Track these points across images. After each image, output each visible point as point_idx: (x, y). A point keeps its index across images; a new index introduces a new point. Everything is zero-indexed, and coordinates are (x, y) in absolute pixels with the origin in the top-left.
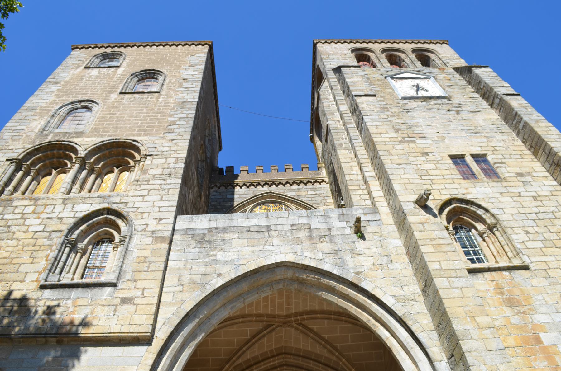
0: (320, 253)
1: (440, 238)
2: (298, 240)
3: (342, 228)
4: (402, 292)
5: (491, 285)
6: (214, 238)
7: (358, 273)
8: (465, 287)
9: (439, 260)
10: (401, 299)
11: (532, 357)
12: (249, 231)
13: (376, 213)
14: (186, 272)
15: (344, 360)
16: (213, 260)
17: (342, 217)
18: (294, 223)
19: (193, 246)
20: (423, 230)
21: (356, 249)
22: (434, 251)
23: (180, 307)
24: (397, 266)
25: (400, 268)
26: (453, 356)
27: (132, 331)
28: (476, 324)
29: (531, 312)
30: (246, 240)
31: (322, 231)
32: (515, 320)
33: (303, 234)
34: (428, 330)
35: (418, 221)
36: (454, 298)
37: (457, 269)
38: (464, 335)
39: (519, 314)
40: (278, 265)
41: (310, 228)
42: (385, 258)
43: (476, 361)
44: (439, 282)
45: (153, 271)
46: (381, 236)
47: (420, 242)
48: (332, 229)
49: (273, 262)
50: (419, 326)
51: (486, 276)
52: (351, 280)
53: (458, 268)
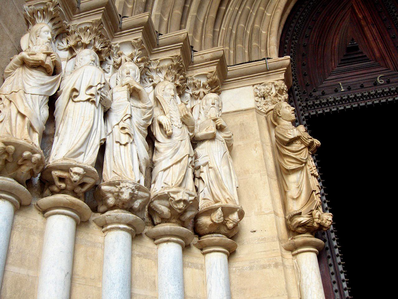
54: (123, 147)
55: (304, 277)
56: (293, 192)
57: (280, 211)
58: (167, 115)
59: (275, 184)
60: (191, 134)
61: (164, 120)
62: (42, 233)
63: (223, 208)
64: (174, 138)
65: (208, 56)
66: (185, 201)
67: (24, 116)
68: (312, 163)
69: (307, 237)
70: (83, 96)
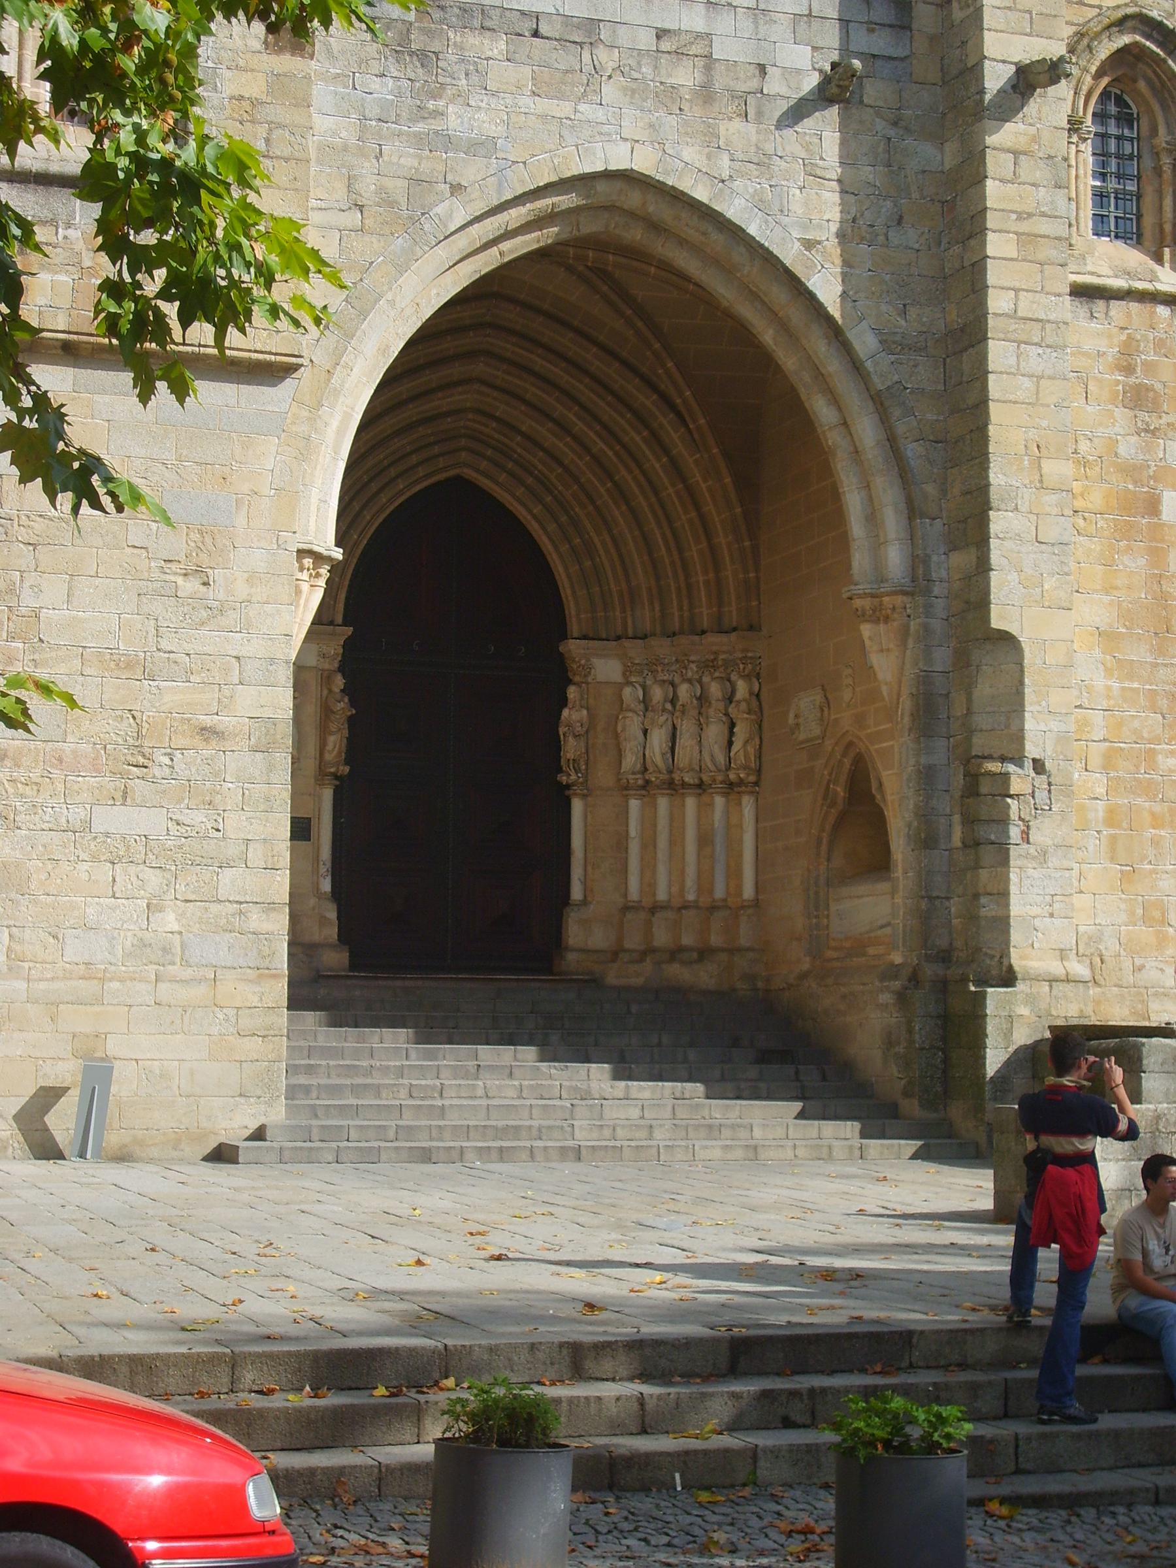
0: (725, 161)
1: (1043, 215)
2: (669, 95)
3: (798, 71)
4: (903, 323)
5: (1116, 341)
6: (436, 46)
7: (809, 244)
8: (1050, 378)
9: (1017, 285)
10: (894, 342)
11: (1123, 543)
12: (536, 34)
13: (902, 27)
14: (366, 164)
15: (670, 364)
16: (436, 132)
17: (803, 25)
18: (667, 26)
19: (376, 67)
20: (1010, 176)
21: (822, 159)
22: (1015, 255)
23: (361, 280)
24: (911, 236)
25: (916, 246)
26: (965, 521)
27: (259, 347)
28: (1037, 477)
29: (1170, 434)
30: (528, 69)
31: (742, 75)
32: (1128, 448)
33: (685, 77)
34: (931, 438)
35: (1009, 144)
36: (1015, 402)
37: (1049, 321)
38: (1002, 500)
39: (1143, 434)
40: (608, 175)
41: (709, 56)
42: (889, 204)
43: (1004, 562)
44: (999, 353)
45: (287, 160)
46: (895, 124)
47: (991, 221)
48: (769, 69)
49: (600, 167)
50: (915, 424)
51: (1112, 313)
52: (787, 262)
53: (1052, 317)
56: (330, 747)
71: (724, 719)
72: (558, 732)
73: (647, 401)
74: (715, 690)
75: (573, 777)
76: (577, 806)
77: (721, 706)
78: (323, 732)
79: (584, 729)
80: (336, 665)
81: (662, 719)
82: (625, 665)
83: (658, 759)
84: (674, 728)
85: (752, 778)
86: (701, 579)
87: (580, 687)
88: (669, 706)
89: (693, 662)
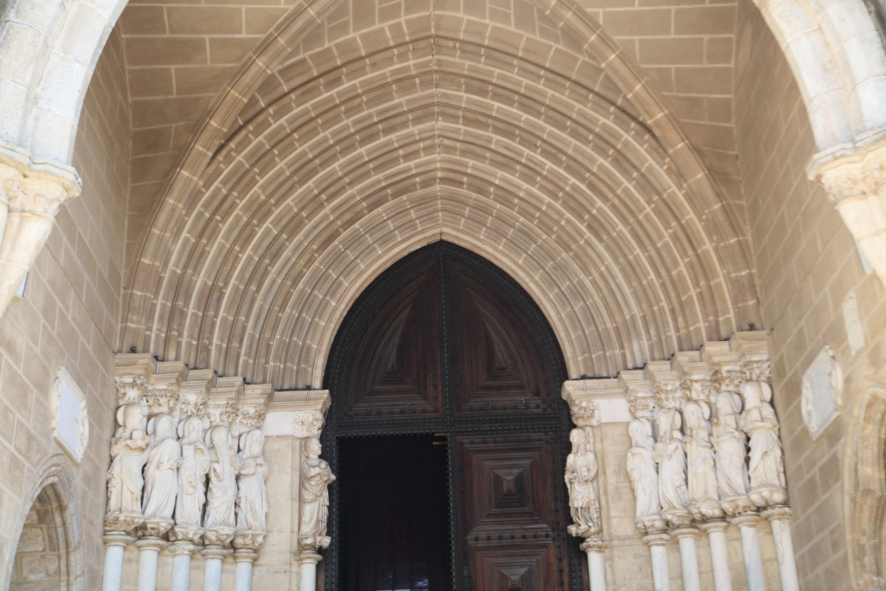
54: (189, 496)
55: (303, 581)
56: (306, 518)
57: (296, 529)
58: (221, 463)
59: (296, 505)
60: (237, 473)
61: (216, 466)
62: (138, 561)
63: (252, 535)
64: (224, 481)
65: (260, 391)
66: (227, 535)
67: (132, 493)
68: (326, 494)
69: (308, 553)
70: (166, 466)
71: (737, 434)
72: (564, 479)
73: (606, 121)
74: (725, 404)
75: (583, 527)
76: (595, 560)
77: (731, 421)
78: (301, 501)
79: (593, 474)
80: (316, 432)
81: (672, 447)
82: (630, 401)
83: (671, 495)
84: (686, 454)
85: (778, 497)
86: (693, 293)
87: (584, 430)
88: (677, 434)
89: (696, 381)
